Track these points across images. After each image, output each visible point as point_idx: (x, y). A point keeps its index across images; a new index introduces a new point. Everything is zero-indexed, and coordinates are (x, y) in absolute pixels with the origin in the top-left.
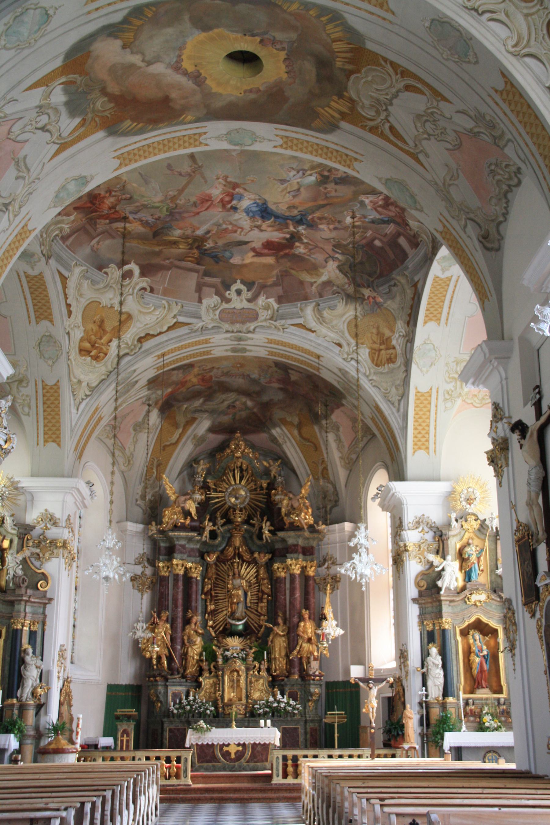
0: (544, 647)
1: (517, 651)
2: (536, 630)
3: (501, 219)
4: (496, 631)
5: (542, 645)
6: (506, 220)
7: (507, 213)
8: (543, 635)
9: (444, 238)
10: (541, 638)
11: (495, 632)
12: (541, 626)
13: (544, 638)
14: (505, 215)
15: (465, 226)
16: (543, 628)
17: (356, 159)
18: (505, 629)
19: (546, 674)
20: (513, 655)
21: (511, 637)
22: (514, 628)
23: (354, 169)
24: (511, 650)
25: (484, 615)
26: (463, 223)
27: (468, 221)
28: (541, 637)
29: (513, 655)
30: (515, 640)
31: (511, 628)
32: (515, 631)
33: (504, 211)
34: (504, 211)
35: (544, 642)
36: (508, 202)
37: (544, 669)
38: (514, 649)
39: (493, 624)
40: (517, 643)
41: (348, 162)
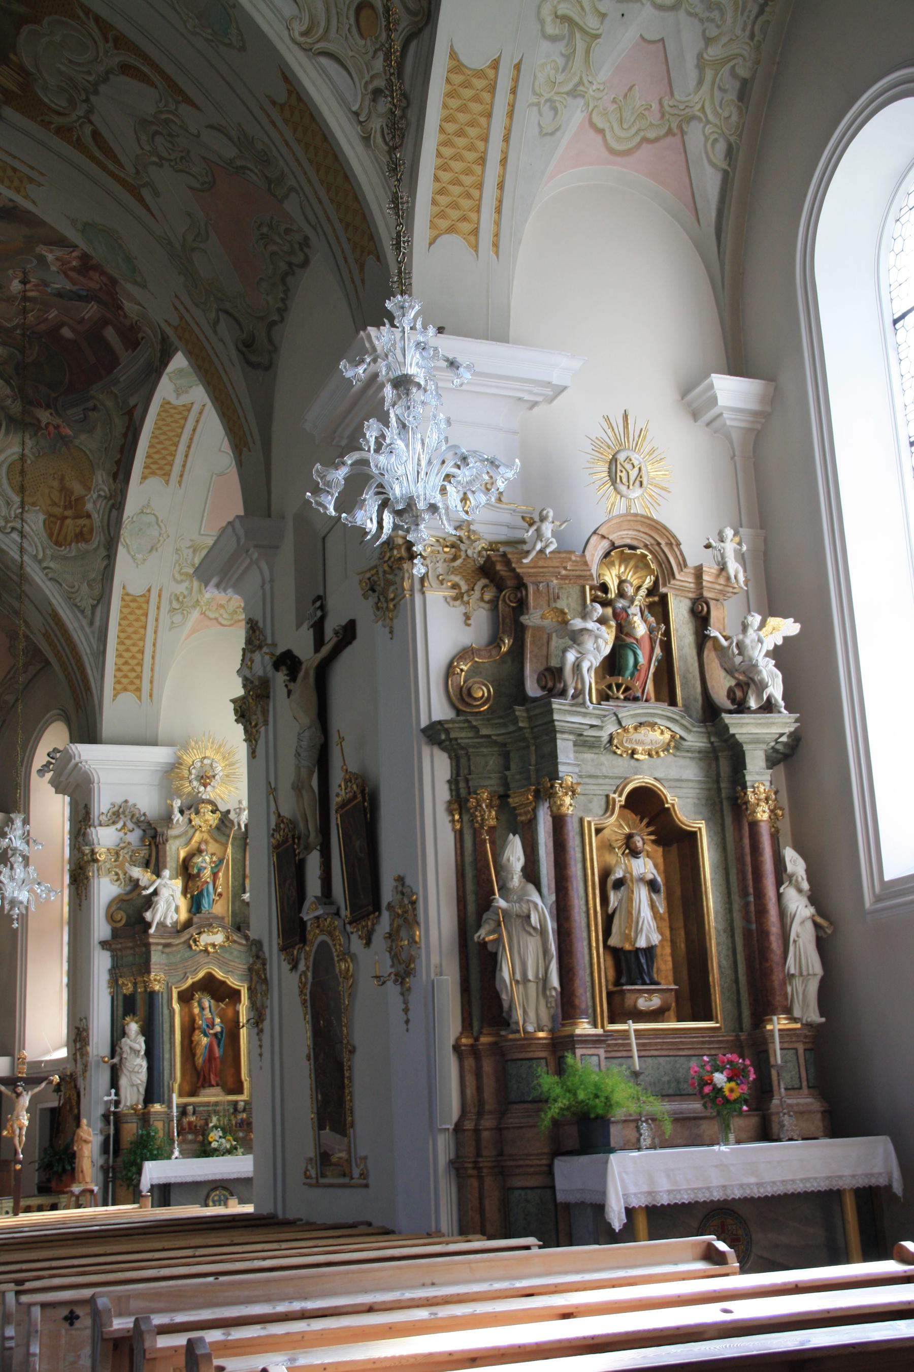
0: (308, 1017)
1: (266, 1025)
2: (297, 991)
3: (276, 318)
4: (238, 992)
5: (305, 1014)
6: (282, 320)
7: (285, 309)
8: (308, 997)
9: (180, 338)
10: (304, 1002)
11: (235, 995)
12: (305, 984)
13: (308, 1004)
14: (283, 311)
15: (217, 322)
16: (309, 986)
17: (31, 180)
18: (249, 989)
19: (309, 1060)
20: (260, 1032)
21: (259, 1003)
22: (264, 987)
23: (26, 197)
24: (257, 1024)
25: (220, 968)
26: (213, 316)
27: (220, 313)
28: (305, 1001)
29: (260, 1032)
30: (264, 1007)
31: (258, 987)
32: (266, 993)
33: (280, 305)
34: (280, 305)
35: (309, 1009)
36: (286, 291)
37: (307, 1051)
38: (262, 1021)
39: (233, 982)
40: (268, 1011)
41: (16, 183)
